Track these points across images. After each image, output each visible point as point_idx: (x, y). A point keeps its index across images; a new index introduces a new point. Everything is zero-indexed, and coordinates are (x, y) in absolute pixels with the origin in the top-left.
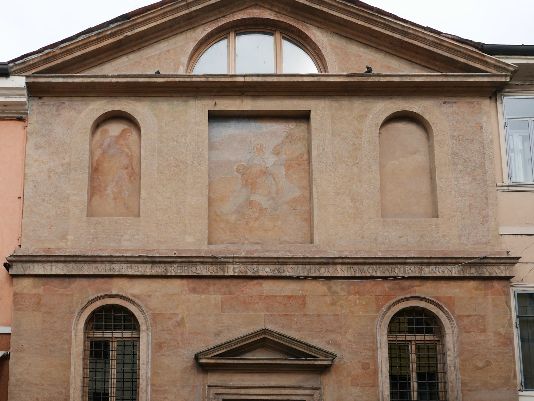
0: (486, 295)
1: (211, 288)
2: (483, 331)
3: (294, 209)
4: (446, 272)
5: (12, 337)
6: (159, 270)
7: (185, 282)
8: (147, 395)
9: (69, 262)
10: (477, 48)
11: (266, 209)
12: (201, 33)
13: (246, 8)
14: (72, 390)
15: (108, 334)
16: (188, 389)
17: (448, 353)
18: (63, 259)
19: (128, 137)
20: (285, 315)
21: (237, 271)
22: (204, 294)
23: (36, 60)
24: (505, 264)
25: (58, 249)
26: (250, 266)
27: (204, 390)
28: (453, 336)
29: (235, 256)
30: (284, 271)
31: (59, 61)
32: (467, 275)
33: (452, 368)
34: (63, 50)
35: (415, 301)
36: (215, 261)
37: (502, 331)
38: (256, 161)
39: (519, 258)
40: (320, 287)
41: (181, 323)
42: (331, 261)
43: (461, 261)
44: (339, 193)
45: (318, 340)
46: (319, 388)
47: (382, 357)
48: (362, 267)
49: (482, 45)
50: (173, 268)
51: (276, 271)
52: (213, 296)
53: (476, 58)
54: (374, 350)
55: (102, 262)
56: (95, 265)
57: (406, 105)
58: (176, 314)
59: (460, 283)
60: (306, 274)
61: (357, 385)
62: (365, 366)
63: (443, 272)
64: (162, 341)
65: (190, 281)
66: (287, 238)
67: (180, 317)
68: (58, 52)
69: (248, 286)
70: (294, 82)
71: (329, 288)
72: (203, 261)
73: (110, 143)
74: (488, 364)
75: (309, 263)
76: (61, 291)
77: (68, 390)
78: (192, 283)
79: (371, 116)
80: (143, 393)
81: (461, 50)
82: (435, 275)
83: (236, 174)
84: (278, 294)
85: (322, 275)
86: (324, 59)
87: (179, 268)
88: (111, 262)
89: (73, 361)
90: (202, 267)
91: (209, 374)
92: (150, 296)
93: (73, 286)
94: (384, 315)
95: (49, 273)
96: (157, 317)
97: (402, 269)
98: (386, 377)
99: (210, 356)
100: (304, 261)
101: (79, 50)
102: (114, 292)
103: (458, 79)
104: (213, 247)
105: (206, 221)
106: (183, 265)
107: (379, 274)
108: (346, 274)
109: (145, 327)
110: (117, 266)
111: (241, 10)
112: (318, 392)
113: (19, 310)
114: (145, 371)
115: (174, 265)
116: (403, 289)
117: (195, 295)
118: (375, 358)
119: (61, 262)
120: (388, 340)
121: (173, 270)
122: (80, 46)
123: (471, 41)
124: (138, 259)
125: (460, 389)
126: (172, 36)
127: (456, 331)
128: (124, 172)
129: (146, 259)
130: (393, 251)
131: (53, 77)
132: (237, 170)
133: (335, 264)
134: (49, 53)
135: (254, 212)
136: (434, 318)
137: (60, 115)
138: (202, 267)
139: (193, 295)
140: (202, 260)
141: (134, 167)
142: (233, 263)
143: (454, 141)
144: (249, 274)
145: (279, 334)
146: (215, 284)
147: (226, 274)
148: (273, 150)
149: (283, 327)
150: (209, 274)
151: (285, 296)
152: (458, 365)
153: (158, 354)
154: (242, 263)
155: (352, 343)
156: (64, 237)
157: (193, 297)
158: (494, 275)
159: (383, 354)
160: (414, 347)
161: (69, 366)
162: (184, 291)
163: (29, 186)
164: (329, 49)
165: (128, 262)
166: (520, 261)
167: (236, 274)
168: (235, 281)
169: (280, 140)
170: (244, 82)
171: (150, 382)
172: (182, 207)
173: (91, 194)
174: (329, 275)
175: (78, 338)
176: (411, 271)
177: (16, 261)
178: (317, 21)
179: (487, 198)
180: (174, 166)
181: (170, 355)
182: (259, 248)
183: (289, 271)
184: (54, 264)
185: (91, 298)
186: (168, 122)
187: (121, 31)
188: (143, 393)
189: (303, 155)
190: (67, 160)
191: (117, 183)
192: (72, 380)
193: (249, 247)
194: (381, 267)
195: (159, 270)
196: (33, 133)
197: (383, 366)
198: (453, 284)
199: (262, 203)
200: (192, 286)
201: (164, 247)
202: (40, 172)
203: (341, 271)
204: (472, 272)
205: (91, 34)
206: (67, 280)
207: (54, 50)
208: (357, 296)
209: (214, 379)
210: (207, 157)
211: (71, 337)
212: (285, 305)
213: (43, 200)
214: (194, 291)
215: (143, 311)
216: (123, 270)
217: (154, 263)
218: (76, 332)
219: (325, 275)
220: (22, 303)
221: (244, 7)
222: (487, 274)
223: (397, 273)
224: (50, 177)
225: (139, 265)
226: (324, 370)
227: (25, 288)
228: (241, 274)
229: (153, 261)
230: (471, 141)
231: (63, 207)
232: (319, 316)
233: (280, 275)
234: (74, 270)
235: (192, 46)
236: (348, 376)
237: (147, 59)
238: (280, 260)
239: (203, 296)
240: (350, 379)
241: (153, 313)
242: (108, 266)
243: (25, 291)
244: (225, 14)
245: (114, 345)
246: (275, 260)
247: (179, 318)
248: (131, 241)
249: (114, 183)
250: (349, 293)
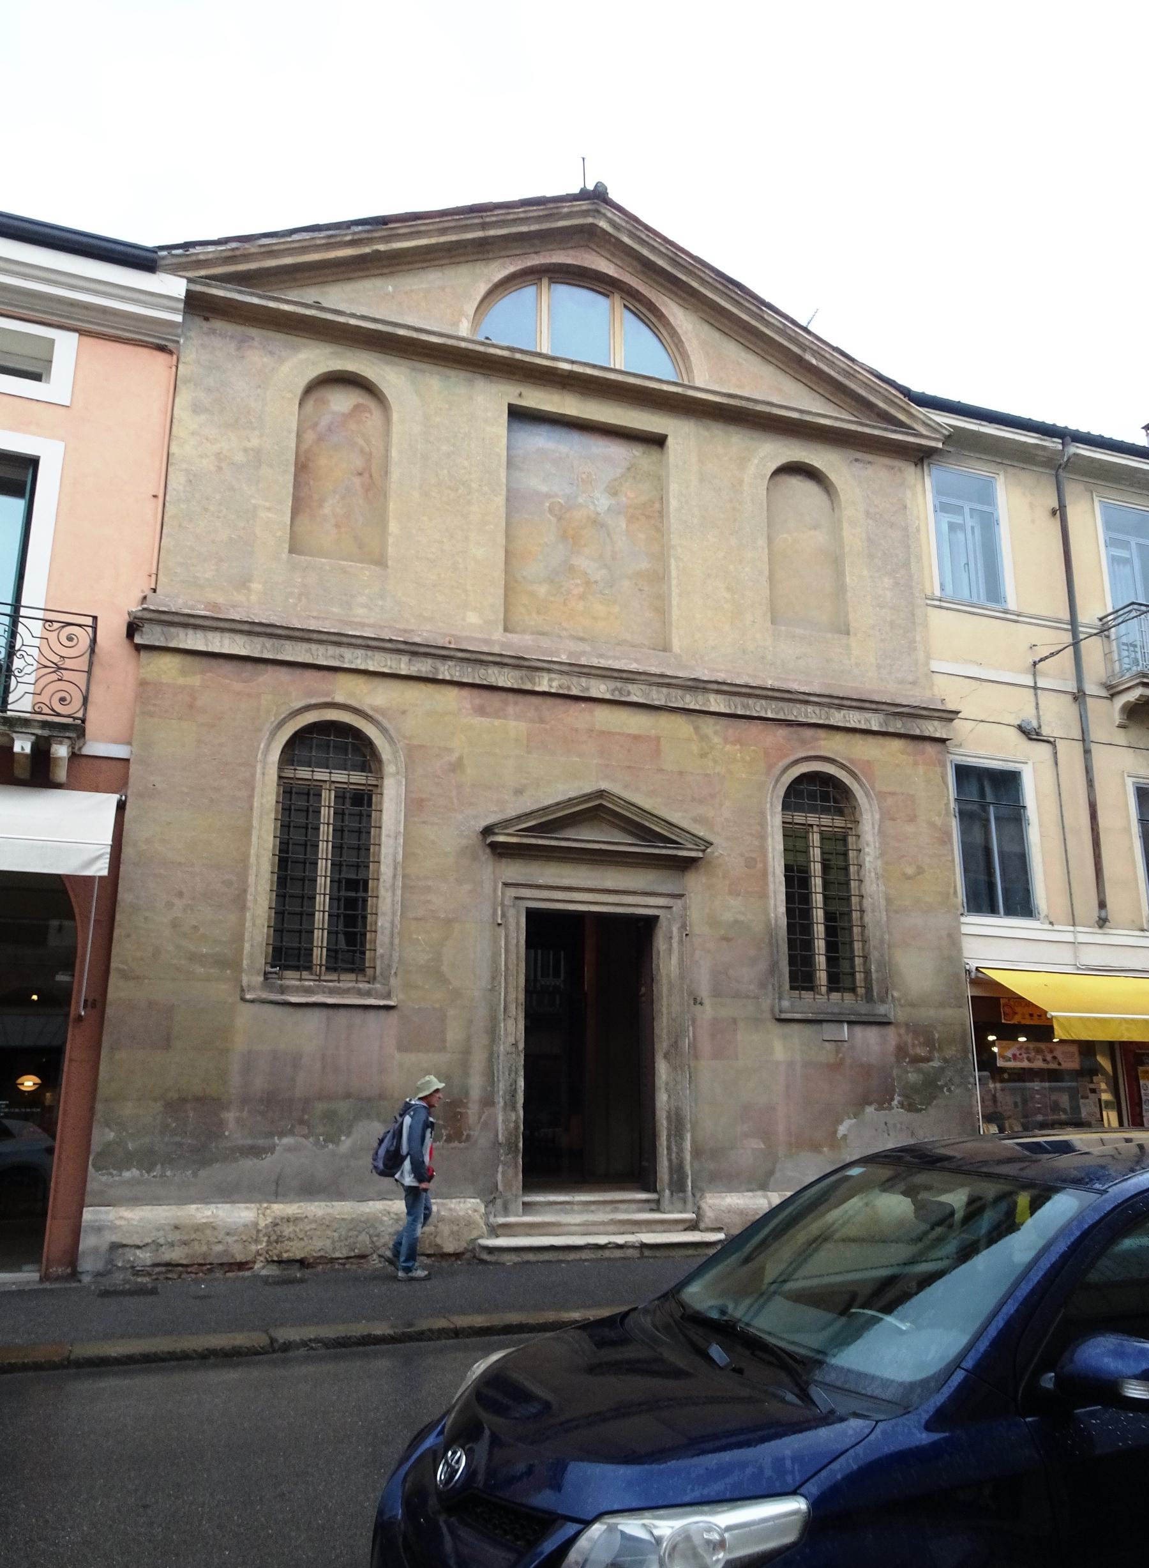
1: (511, 710)
2: (912, 819)
3: (640, 590)
4: (863, 722)
5: (133, 768)
6: (423, 667)
7: (465, 693)
8: (394, 895)
9: (259, 634)
10: (901, 392)
11: (596, 582)
12: (499, 271)
13: (572, 248)
14: (251, 879)
15: (321, 775)
16: (467, 887)
17: (867, 850)
18: (246, 627)
19: (364, 419)
20: (629, 767)
21: (555, 684)
22: (499, 718)
23: (210, 256)
24: (940, 719)
25: (234, 607)
26: (575, 680)
27: (495, 890)
28: (873, 824)
29: (554, 659)
30: (629, 693)
31: (253, 266)
32: (891, 730)
33: (873, 874)
34: (263, 250)
35: (820, 763)
36: (518, 663)
37: (938, 821)
38: (580, 500)
39: (959, 712)
40: (681, 726)
41: (457, 766)
42: (702, 685)
43: (884, 707)
44: (709, 575)
45: (680, 814)
46: (680, 896)
47: (773, 849)
48: (745, 700)
50: (446, 667)
51: (617, 692)
52: (513, 724)
53: (901, 407)
54: (762, 837)
55: (320, 642)
56: (305, 646)
57: (804, 454)
58: (450, 750)
60: (662, 703)
61: (738, 895)
62: (750, 863)
63: (859, 721)
64: (424, 796)
65: (476, 692)
66: (628, 637)
67: (456, 755)
68: (253, 250)
69: (571, 712)
71: (697, 729)
72: (500, 662)
74: (920, 871)
75: (669, 685)
76: (238, 686)
77: (243, 877)
78: (479, 697)
79: (756, 461)
80: (387, 890)
81: (882, 391)
82: (848, 725)
83: (549, 516)
84: (618, 731)
85: (687, 707)
86: (689, 356)
87: (458, 669)
88: (339, 644)
89: (255, 823)
90: (496, 672)
91: (504, 860)
92: (404, 712)
93: (261, 679)
94: (777, 781)
95: (217, 650)
96: (413, 754)
97: (803, 710)
98: (780, 882)
99: (510, 831)
100: (661, 680)
101: (291, 255)
102: (339, 699)
103: (876, 432)
104: (513, 638)
105: (501, 591)
106: (465, 665)
107: (770, 715)
108: (723, 709)
109: (394, 768)
110: (348, 653)
111: (564, 249)
112: (679, 902)
113: (151, 714)
114: (391, 851)
115: (450, 663)
116: (803, 742)
117: (483, 719)
118: (763, 850)
119: (241, 632)
120: (783, 822)
121: (445, 671)
122: (295, 248)
124: (389, 645)
125: (883, 907)
126: (450, 264)
127: (877, 816)
128: (357, 481)
129: (402, 647)
130: (788, 680)
131: (240, 292)
132: (551, 510)
133: (706, 690)
134: (237, 249)
135: (577, 585)
136: (845, 792)
138: (496, 672)
139: (479, 719)
140: (498, 659)
141: (375, 475)
142: (549, 670)
143: (870, 522)
144: (575, 692)
145: (625, 801)
146: (516, 703)
147: (537, 689)
148: (608, 487)
149: (626, 787)
150: (509, 685)
151: (629, 735)
152: (879, 871)
153: (416, 819)
154: (562, 672)
155: (731, 824)
156: (243, 583)
157: (478, 721)
158: (927, 734)
159: (776, 844)
160: (817, 837)
161: (248, 831)
162: (464, 711)
163: (177, 481)
164: (695, 343)
165: (368, 647)
166: (960, 715)
167: (553, 691)
168: (550, 701)
169: (619, 472)
171: (399, 869)
172: (460, 560)
173: (295, 512)
174: (698, 707)
175: (266, 778)
176: (812, 715)
177: (150, 620)
178: (680, 297)
180: (449, 488)
181: (437, 824)
182: (588, 649)
183: (636, 694)
184: (227, 635)
185: (298, 705)
188: (387, 890)
189: (654, 503)
190: (255, 442)
191: (343, 498)
192: (253, 860)
193: (572, 646)
194: (774, 704)
195: (423, 667)
197: (776, 864)
199: (589, 571)
200: (477, 701)
201: (428, 627)
202: (201, 456)
203: (717, 704)
204: (897, 726)
206: (249, 667)
207: (247, 246)
208: (738, 747)
209: (514, 870)
210: (504, 480)
211: (253, 775)
212: (629, 751)
213: (206, 510)
214: (481, 711)
215: (391, 738)
216: (359, 661)
217: (414, 654)
218: (264, 768)
219: (692, 707)
220: (158, 702)
221: (569, 246)
223: (796, 717)
224: (220, 468)
225: (388, 656)
226: (686, 865)
227: (165, 673)
228: (561, 692)
229: (414, 650)
230: (892, 525)
231: (244, 528)
232: (681, 773)
233: (623, 699)
234: (265, 651)
235: (483, 288)
236: (724, 877)
237: (406, 293)
238: (624, 675)
239: (497, 722)
240: (727, 882)
241: (408, 744)
242: (332, 650)
243: (165, 679)
244: (538, 249)
245: (328, 798)
246: (616, 674)
247: (454, 757)
248: (370, 609)
250: (726, 741)
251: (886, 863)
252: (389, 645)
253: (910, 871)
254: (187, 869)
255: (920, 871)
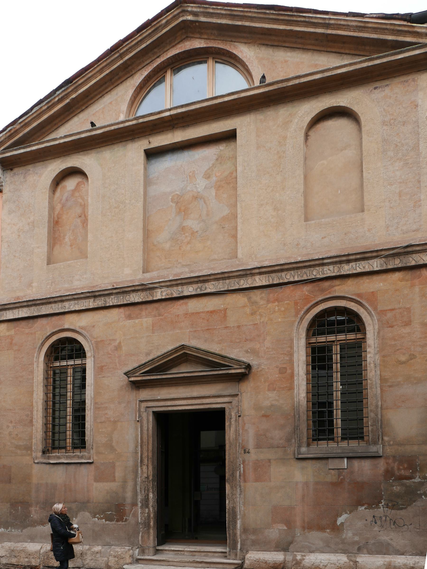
0: (413, 286)
1: (144, 313)
2: (408, 323)
3: (223, 228)
4: (367, 267)
6: (99, 303)
7: (122, 310)
10: (405, 20)
13: (178, 43)
14: (35, 413)
16: (123, 405)
18: (25, 304)
20: (208, 329)
21: (164, 294)
26: (175, 288)
28: (374, 332)
30: (206, 289)
31: (21, 135)
32: (390, 267)
33: (372, 365)
34: (22, 124)
38: (188, 188)
41: (118, 348)
42: (248, 272)
43: (383, 253)
44: (262, 205)
45: (238, 350)
46: (237, 395)
48: (279, 274)
49: (411, 15)
51: (199, 289)
52: (145, 320)
53: (406, 32)
55: (55, 302)
56: (50, 306)
58: (114, 340)
59: (384, 277)
60: (226, 289)
61: (274, 390)
62: (282, 371)
64: (103, 364)
65: (126, 308)
66: (216, 257)
67: (118, 342)
69: (175, 307)
70: (216, 105)
71: (249, 299)
73: (68, 197)
75: (229, 278)
76: (27, 331)
79: (296, 121)
81: (388, 27)
82: (355, 272)
83: (171, 203)
84: (201, 311)
85: (241, 287)
88: (62, 301)
89: (35, 389)
90: (134, 295)
91: (141, 390)
92: (94, 326)
93: (36, 325)
94: (302, 319)
98: (303, 380)
99: (137, 374)
100: (223, 276)
101: (35, 121)
102: (66, 327)
103: (385, 60)
104: (148, 275)
106: (119, 296)
107: (296, 279)
108: (264, 283)
110: (66, 304)
111: (173, 46)
112: (236, 399)
115: (112, 297)
116: (323, 290)
117: (130, 321)
118: (291, 362)
121: (112, 301)
123: (398, 14)
124: (82, 296)
126: (114, 87)
127: (377, 327)
128: (79, 220)
129: (88, 295)
131: (16, 150)
132: (172, 200)
133: (253, 275)
134: (11, 130)
135: (187, 236)
137: (26, 181)
140: (133, 288)
143: (385, 127)
144: (175, 295)
146: (146, 309)
147: (155, 299)
150: (140, 300)
151: (208, 312)
153: (100, 376)
154: (168, 286)
155: (270, 350)
156: (30, 285)
162: (121, 319)
165: (74, 299)
167: (163, 297)
168: (164, 304)
170: (171, 116)
174: (248, 286)
179: (419, 182)
180: (116, 208)
181: (109, 377)
183: (210, 287)
184: (20, 309)
185: (48, 334)
186: (110, 168)
187: (67, 95)
190: (32, 219)
191: (73, 231)
192: (34, 404)
194: (299, 272)
195: (99, 303)
196: (7, 201)
197: (300, 369)
198: (376, 278)
204: (397, 263)
205: (42, 105)
206: (31, 321)
207: (14, 126)
208: (276, 303)
209: (145, 394)
213: (15, 256)
214: (129, 317)
216: (72, 307)
217: (95, 297)
218: (38, 364)
219: (244, 286)
221: (176, 42)
222: (413, 263)
223: (315, 275)
224: (19, 236)
227: (2, 332)
228: (168, 297)
233: (202, 292)
234: (35, 312)
237: (93, 114)
238: (201, 279)
239: (137, 321)
240: (267, 384)
241: (96, 341)
242: (60, 305)
244: (158, 55)
246: (196, 280)
247: (116, 343)
248: (81, 280)
249: (71, 232)
251: (384, 356)
252: (82, 296)
253: (403, 358)
254: (13, 412)
255: (412, 357)
